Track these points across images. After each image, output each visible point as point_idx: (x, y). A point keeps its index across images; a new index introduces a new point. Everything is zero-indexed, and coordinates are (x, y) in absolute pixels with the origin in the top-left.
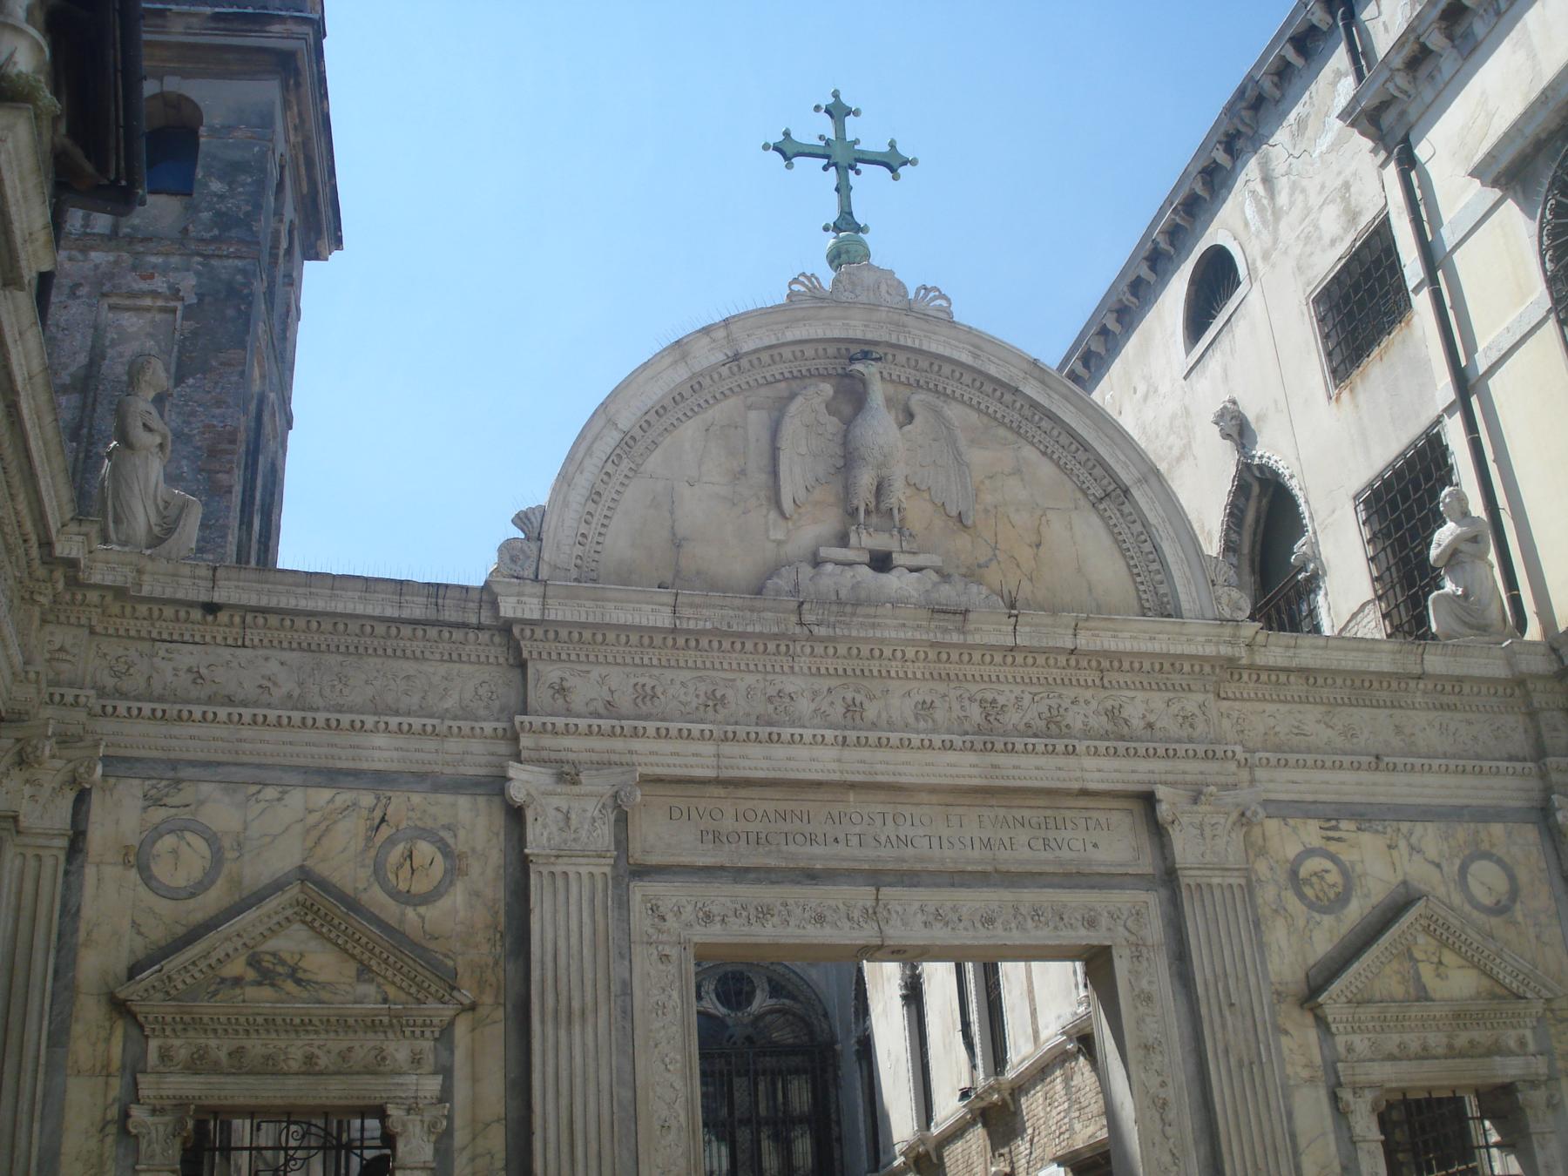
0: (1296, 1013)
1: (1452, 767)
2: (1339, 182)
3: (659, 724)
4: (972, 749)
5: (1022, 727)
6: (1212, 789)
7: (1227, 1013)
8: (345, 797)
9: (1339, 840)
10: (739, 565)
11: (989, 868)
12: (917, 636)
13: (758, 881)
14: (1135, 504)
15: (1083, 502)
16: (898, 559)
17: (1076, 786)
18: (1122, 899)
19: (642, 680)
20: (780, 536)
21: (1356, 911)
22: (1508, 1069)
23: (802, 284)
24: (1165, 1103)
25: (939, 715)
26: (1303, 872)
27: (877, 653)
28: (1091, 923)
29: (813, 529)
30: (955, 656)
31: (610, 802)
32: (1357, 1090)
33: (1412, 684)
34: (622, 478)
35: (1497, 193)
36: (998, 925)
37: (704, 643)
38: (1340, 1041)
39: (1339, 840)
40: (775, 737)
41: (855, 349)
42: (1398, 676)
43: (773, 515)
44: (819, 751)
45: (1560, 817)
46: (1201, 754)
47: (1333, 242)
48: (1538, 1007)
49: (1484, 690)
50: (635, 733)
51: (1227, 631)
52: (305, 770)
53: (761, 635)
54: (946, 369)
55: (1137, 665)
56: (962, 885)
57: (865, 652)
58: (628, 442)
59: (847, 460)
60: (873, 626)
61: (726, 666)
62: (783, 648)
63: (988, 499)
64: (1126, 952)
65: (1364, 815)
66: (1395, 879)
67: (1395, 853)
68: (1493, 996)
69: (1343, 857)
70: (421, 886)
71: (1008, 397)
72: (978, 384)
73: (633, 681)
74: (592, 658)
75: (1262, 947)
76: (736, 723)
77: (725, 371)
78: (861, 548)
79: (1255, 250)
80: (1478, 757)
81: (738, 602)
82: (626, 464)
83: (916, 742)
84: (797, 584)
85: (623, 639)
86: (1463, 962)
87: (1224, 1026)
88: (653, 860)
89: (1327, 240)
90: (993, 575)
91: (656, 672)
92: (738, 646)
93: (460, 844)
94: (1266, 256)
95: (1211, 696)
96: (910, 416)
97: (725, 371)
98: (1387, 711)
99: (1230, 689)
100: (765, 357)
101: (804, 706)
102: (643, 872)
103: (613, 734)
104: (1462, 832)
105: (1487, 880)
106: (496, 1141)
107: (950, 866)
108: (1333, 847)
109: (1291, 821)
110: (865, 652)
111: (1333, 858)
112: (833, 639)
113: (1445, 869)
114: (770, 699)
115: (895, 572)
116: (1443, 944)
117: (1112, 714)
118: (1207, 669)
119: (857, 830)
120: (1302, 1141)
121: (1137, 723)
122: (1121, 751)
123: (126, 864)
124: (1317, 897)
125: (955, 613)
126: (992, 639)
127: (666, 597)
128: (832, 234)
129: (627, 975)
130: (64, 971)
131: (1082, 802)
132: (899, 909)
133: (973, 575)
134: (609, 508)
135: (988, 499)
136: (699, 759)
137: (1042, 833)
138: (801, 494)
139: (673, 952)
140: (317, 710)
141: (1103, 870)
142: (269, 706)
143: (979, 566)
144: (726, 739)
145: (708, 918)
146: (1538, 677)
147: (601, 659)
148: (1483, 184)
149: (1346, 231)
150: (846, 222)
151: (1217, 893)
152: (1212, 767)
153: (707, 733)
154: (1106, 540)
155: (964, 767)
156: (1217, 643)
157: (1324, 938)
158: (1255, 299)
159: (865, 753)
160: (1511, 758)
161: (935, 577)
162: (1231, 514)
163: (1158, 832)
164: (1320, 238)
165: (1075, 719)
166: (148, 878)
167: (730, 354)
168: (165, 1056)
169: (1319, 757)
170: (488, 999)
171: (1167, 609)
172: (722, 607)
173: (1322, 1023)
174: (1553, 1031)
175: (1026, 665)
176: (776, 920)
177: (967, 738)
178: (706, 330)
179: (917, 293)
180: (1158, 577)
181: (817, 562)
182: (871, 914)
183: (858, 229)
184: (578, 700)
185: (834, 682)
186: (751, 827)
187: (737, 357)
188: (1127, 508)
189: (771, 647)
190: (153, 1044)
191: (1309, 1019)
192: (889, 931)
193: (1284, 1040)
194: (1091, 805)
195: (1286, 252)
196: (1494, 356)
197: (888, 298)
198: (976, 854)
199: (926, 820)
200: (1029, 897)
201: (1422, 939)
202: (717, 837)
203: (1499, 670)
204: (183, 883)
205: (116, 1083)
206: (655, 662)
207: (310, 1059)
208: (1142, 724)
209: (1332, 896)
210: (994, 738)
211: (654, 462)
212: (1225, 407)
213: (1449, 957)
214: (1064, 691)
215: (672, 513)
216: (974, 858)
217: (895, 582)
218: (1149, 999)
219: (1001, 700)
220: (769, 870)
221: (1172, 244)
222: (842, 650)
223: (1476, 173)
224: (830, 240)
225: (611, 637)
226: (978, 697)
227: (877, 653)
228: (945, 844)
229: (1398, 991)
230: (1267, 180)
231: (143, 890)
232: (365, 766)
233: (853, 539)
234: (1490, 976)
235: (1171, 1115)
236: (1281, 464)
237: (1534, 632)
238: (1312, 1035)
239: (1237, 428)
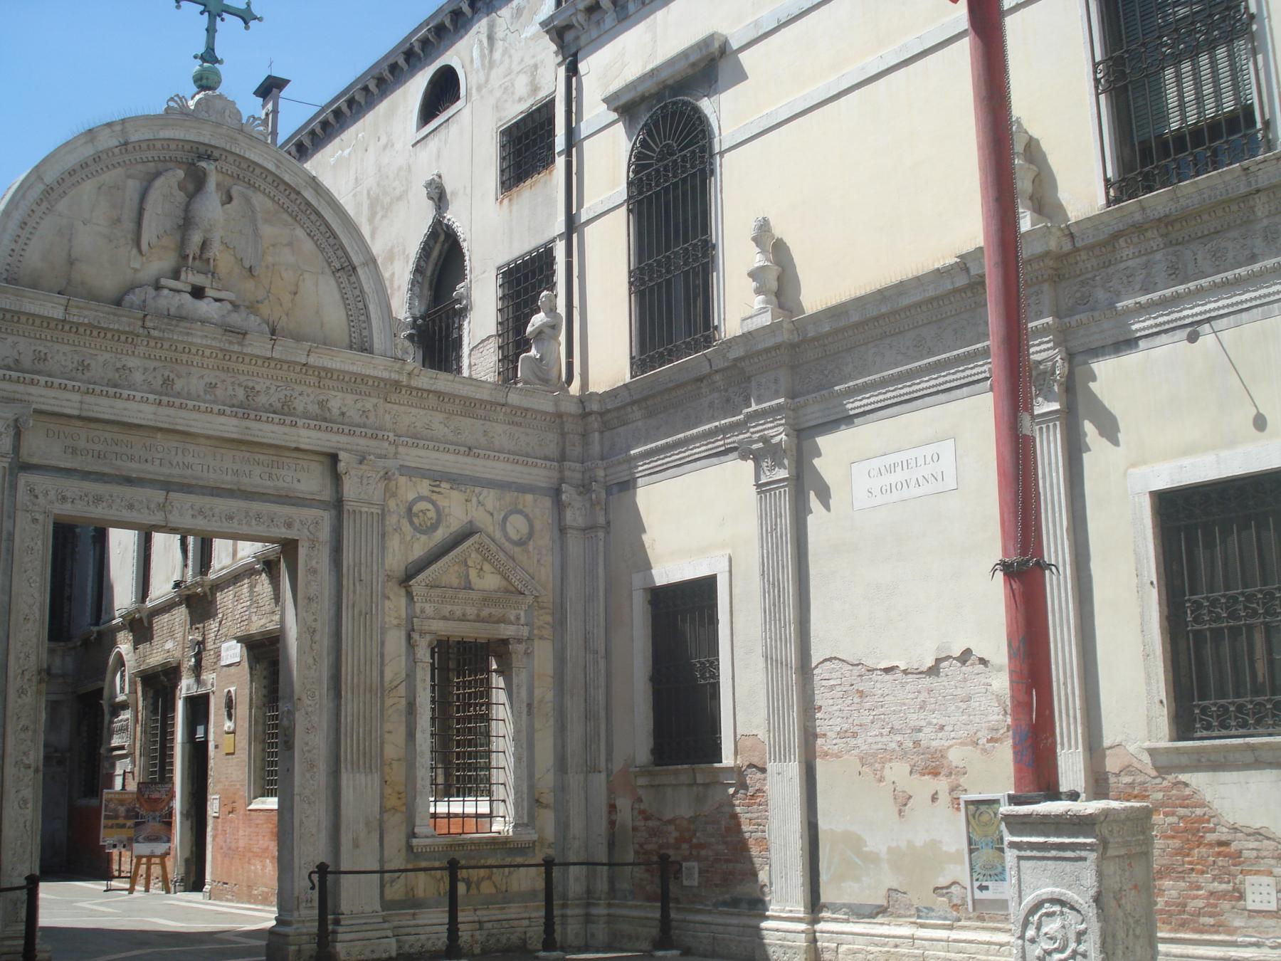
0: (396, 588)
1: (511, 460)
2: (532, 62)
3: (48, 379)
4: (235, 416)
5: (267, 406)
6: (372, 457)
7: (357, 584)
9: (439, 493)
10: (108, 282)
11: (235, 487)
12: (214, 343)
13: (96, 481)
14: (358, 278)
15: (327, 270)
16: (209, 292)
17: (294, 445)
19: (39, 348)
20: (137, 266)
21: (440, 535)
22: (507, 631)
23: (176, 102)
24: (314, 631)
25: (219, 392)
26: (415, 509)
27: (187, 350)
28: (289, 525)
29: (159, 263)
30: (234, 358)
31: (12, 424)
32: (422, 634)
33: (499, 408)
34: (40, 214)
35: (615, 116)
36: (235, 521)
37: (81, 330)
38: (418, 606)
39: (439, 493)
40: (118, 395)
41: (202, 150)
42: (491, 403)
43: (135, 251)
44: (144, 407)
45: (564, 497)
46: (369, 435)
47: (520, 100)
48: (530, 600)
49: (539, 417)
50: (32, 382)
51: (398, 365)
53: (118, 331)
54: (258, 171)
55: (341, 377)
56: (217, 496)
57: (180, 347)
58: (49, 190)
59: (186, 223)
60: (188, 334)
61: (93, 346)
62: (130, 340)
63: (270, 259)
64: (306, 544)
65: (456, 481)
66: (466, 519)
68: (507, 591)
69: (440, 503)
71: (293, 196)
72: (275, 184)
73: (33, 348)
74: (9, 331)
75: (383, 548)
76: (95, 383)
77: (117, 151)
78: (186, 283)
79: (473, 81)
80: (528, 456)
81: (106, 309)
82: (45, 204)
83: (203, 408)
84: (144, 301)
85: (31, 321)
86: (493, 570)
87: (354, 592)
88: (35, 461)
89: (516, 97)
90: (265, 310)
91: (49, 344)
92: (102, 335)
94: (479, 89)
95: (382, 400)
96: (230, 199)
97: (117, 151)
98: (482, 422)
99: (394, 397)
100: (144, 146)
101: (138, 377)
102: (27, 467)
103: (18, 381)
104: (509, 497)
105: (517, 525)
107: (212, 484)
108: (435, 497)
109: (413, 479)
110: (180, 347)
111: (434, 503)
112: (162, 339)
113: (495, 516)
114: (117, 370)
115: (206, 300)
116: (485, 559)
118: (382, 384)
119: (159, 456)
120: (387, 659)
121: (335, 412)
122: (323, 428)
125: (238, 333)
126: (258, 352)
127: (62, 300)
128: (199, 62)
129: (11, 529)
131: (295, 455)
132: (179, 506)
133: (253, 308)
134: (31, 233)
135: (270, 259)
136: (69, 402)
138: (154, 241)
139: (41, 517)
141: (301, 495)
143: (257, 302)
144: (88, 393)
145: (64, 499)
146: (571, 415)
147: (15, 332)
148: (608, 108)
149: (529, 96)
150: (209, 56)
151: (364, 516)
152: (373, 443)
153: (77, 388)
154: (337, 296)
155: (229, 426)
156: (391, 372)
157: (419, 549)
158: (466, 112)
159: (171, 411)
160: (546, 458)
161: (229, 307)
162: (423, 249)
163: (337, 478)
164: (513, 93)
165: (299, 405)
167: (122, 141)
169: (437, 444)
171: (365, 347)
172: (96, 311)
173: (409, 595)
174: (536, 613)
175: (275, 368)
176: (104, 504)
177: (234, 409)
178: (109, 125)
179: (248, 120)
180: (364, 325)
181: (158, 287)
182: (162, 507)
183: (216, 61)
185: (157, 364)
186: (96, 447)
187: (126, 144)
188: (353, 279)
189: (123, 338)
191: (403, 592)
192: (171, 518)
193: (387, 602)
194: (301, 456)
195: (491, 92)
196: (592, 215)
197: (229, 120)
198: (229, 478)
199: (202, 455)
200: (256, 506)
201: (474, 555)
202: (74, 451)
203: (548, 406)
206: (49, 338)
208: (338, 412)
210: (249, 412)
211: (63, 205)
212: (433, 179)
213: (487, 567)
214: (295, 387)
215: (70, 240)
216: (228, 480)
217: (205, 308)
218: (315, 572)
219: (258, 388)
220: (104, 474)
221: (423, 50)
222: (166, 345)
223: (605, 100)
224: (196, 66)
225: (23, 319)
226: (244, 384)
227: (187, 350)
228: (211, 470)
229: (455, 581)
230: (491, 38)
233: (183, 276)
234: (507, 579)
235: (317, 638)
236: (460, 229)
237: (575, 389)
238: (403, 601)
239: (439, 195)
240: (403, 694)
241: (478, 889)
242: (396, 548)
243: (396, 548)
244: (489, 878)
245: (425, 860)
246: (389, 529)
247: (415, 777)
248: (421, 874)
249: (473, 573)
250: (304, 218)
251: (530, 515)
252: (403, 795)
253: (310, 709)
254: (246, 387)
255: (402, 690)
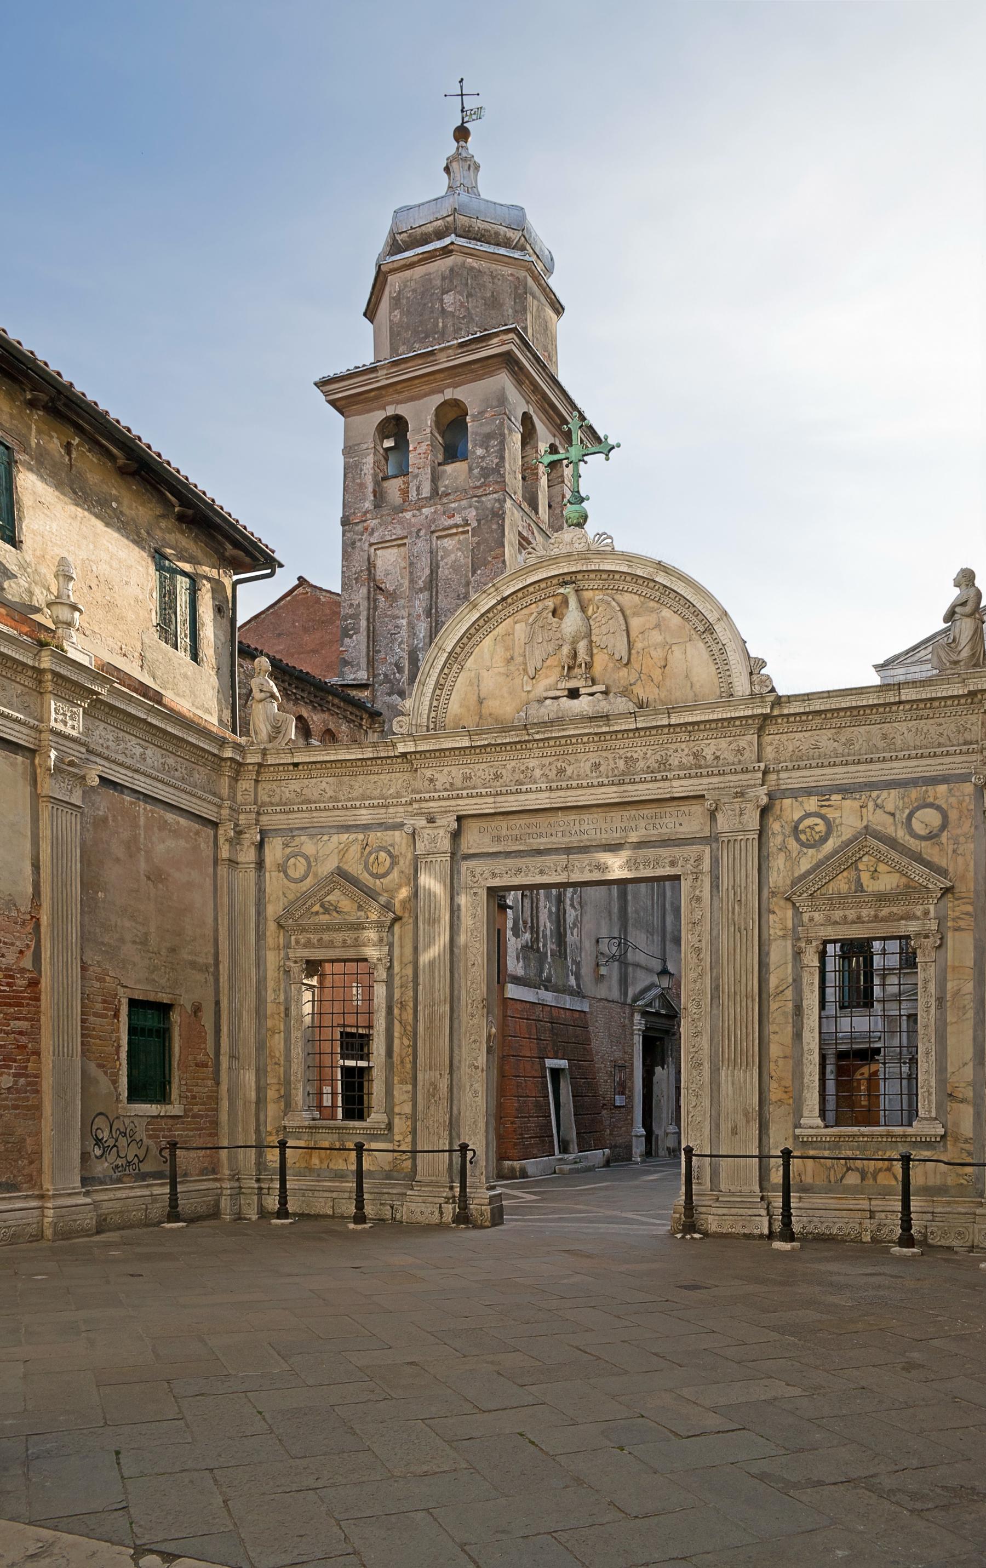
0: (782, 903)
4: (613, 784)
8: (353, 836)
15: (695, 636)
16: (582, 691)
18: (691, 851)
19: (465, 771)
20: (529, 688)
26: (801, 827)
28: (673, 864)
38: (806, 917)
52: (337, 827)
65: (845, 790)
67: (864, 810)
70: (381, 870)
88: (472, 851)
91: (471, 766)
93: (396, 853)
102: (467, 857)
106: (409, 971)
107: (604, 842)
108: (824, 811)
111: (823, 817)
114: (523, 772)
117: (696, 755)
120: (772, 967)
123: (279, 871)
124: (808, 840)
125: (602, 717)
130: (260, 912)
137: (653, 821)
139: (479, 891)
140: (340, 801)
142: (324, 802)
154: (705, 655)
155: (611, 794)
159: (562, 793)
166: (287, 875)
168: (297, 942)
170: (407, 915)
174: (950, 905)
184: (439, 785)
186: (514, 833)
190: (293, 938)
191: (789, 905)
198: (618, 835)
199: (595, 821)
202: (499, 839)
204: (298, 876)
205: (282, 952)
207: (345, 941)
208: (713, 757)
209: (817, 838)
214: (669, 746)
217: (583, 705)
219: (635, 756)
228: (603, 831)
231: (285, 880)
232: (359, 823)
240: (790, 998)
241: (875, 1179)
242: (782, 867)
243: (782, 867)
244: (889, 1169)
245: (815, 1149)
246: (773, 849)
247: (802, 1073)
248: (810, 1162)
249: (865, 877)
250: (666, 600)
251: (944, 806)
252: (790, 1089)
253: (696, 1016)
254: (626, 757)
255: (789, 993)
